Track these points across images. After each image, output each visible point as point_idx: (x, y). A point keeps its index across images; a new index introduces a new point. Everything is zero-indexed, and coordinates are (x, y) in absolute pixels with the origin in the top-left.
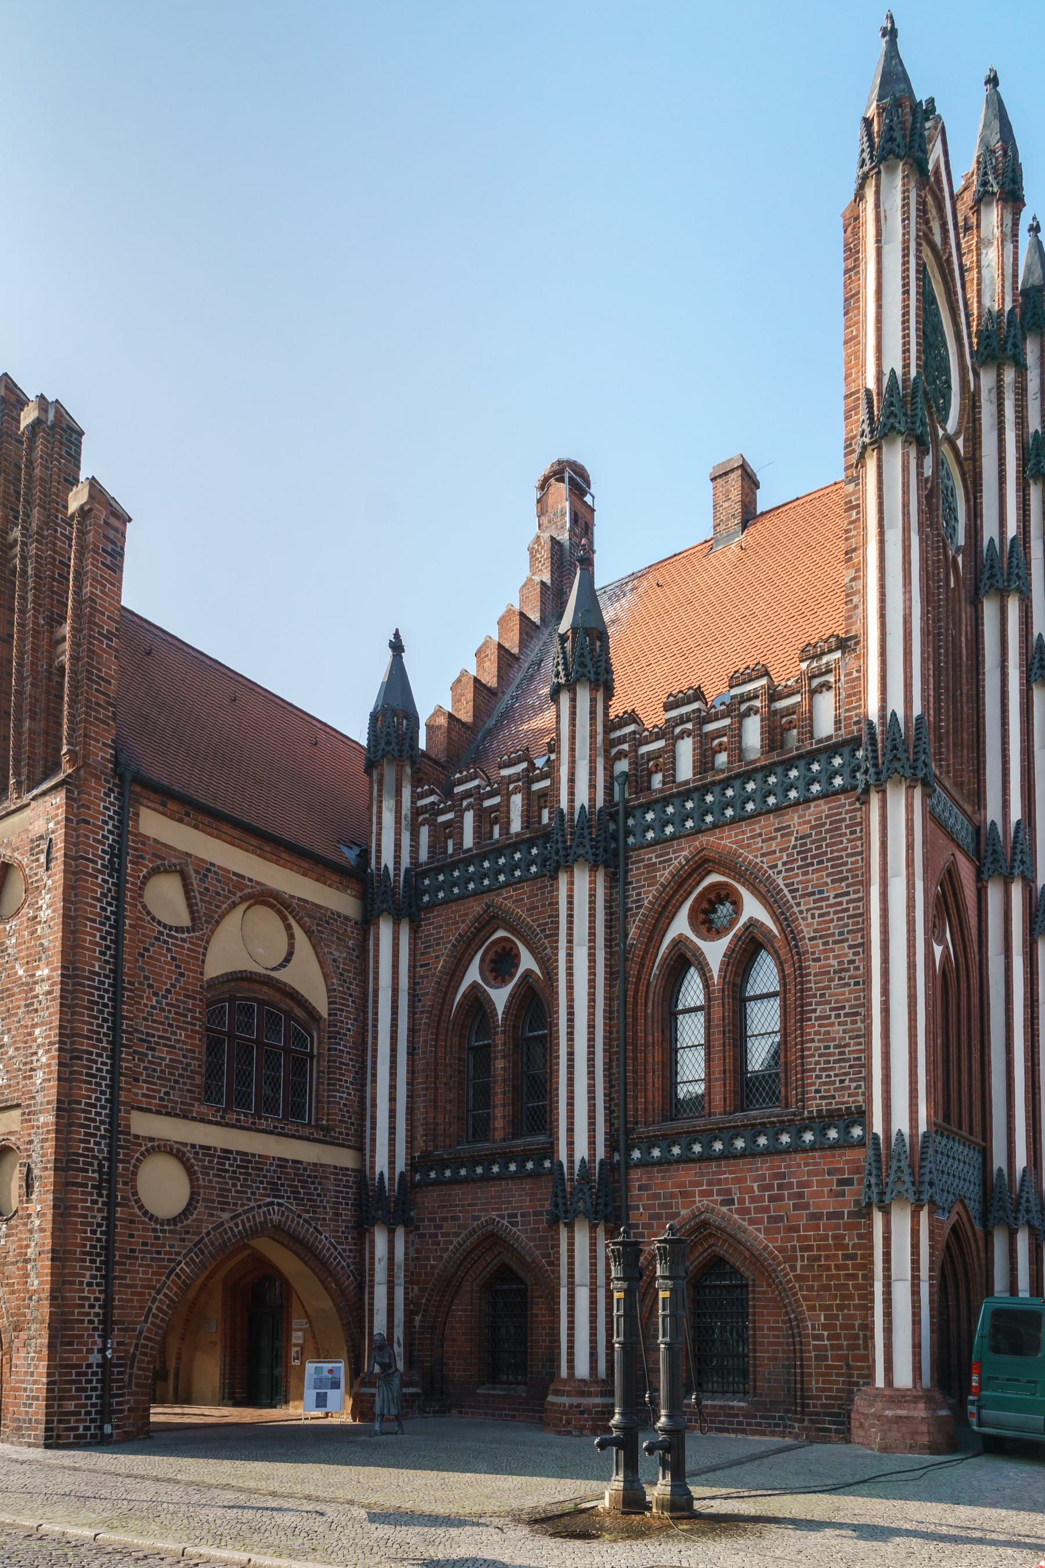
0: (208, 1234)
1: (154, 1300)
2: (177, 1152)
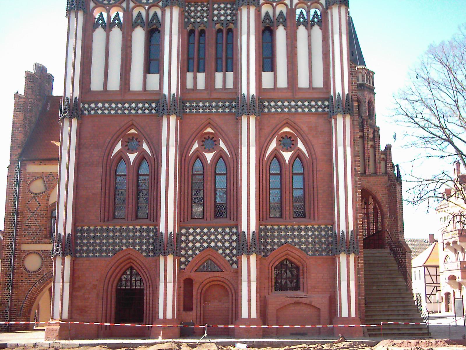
0: (46, 274)
1: (28, 293)
2: (37, 253)
